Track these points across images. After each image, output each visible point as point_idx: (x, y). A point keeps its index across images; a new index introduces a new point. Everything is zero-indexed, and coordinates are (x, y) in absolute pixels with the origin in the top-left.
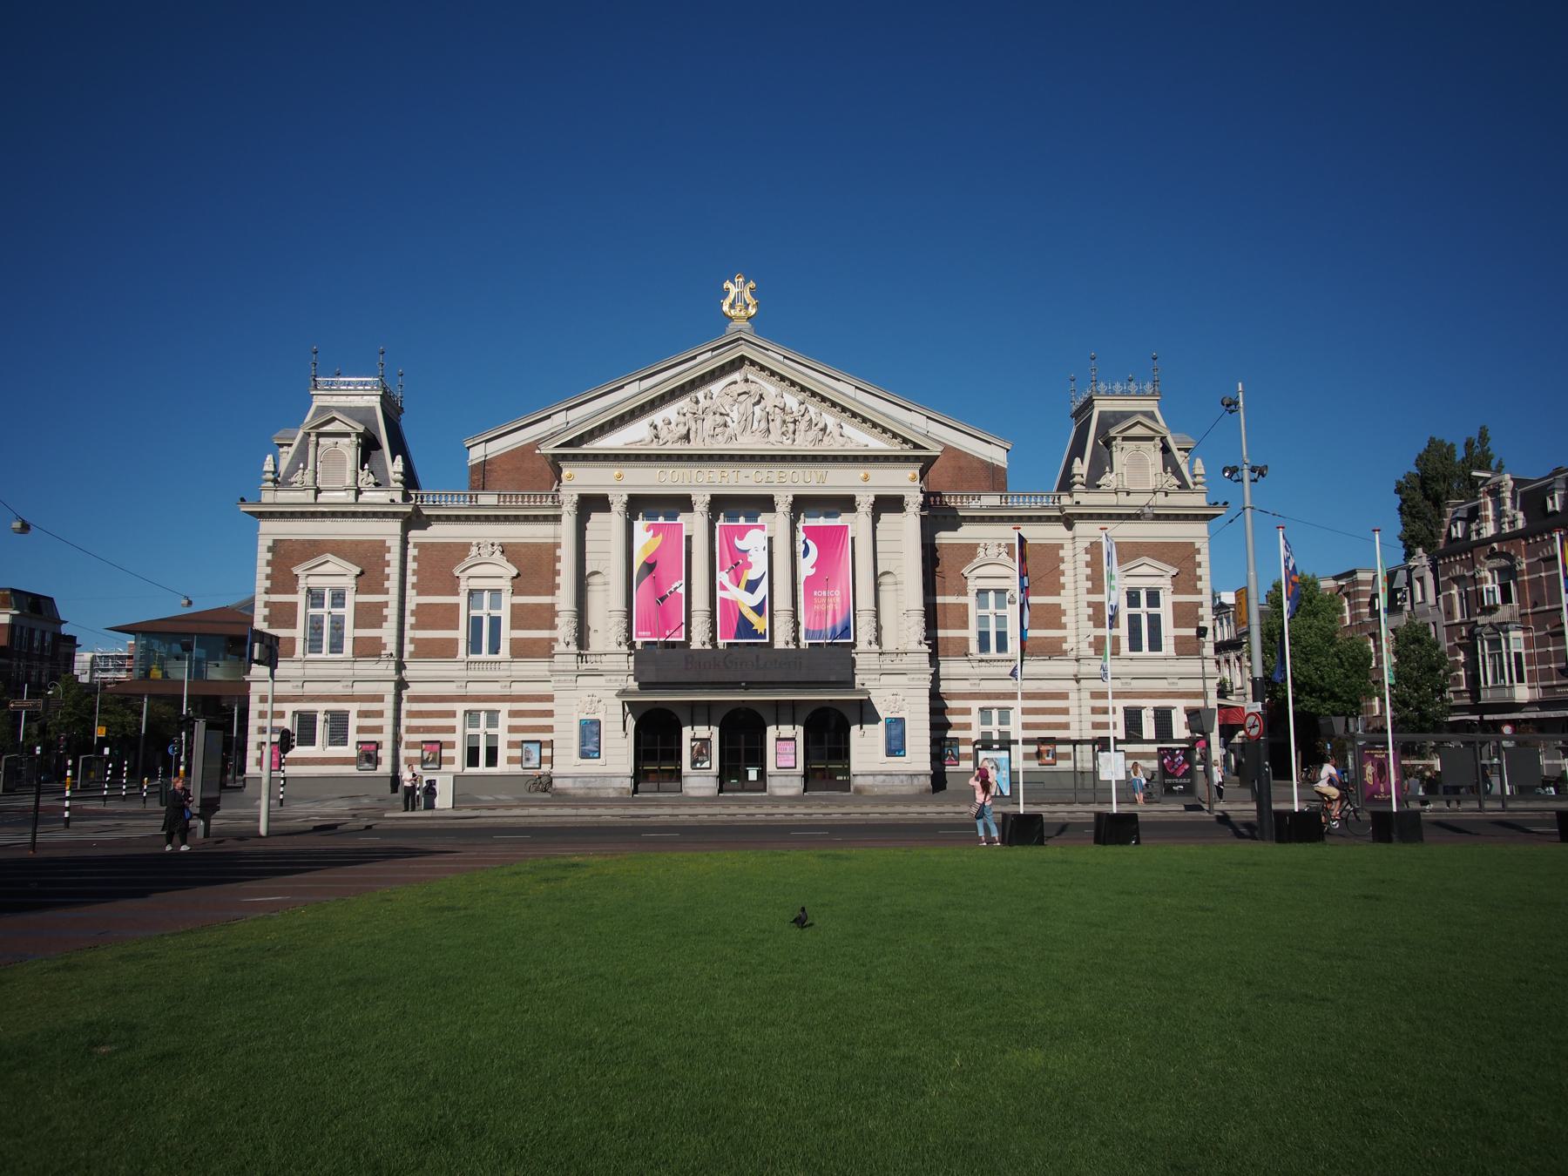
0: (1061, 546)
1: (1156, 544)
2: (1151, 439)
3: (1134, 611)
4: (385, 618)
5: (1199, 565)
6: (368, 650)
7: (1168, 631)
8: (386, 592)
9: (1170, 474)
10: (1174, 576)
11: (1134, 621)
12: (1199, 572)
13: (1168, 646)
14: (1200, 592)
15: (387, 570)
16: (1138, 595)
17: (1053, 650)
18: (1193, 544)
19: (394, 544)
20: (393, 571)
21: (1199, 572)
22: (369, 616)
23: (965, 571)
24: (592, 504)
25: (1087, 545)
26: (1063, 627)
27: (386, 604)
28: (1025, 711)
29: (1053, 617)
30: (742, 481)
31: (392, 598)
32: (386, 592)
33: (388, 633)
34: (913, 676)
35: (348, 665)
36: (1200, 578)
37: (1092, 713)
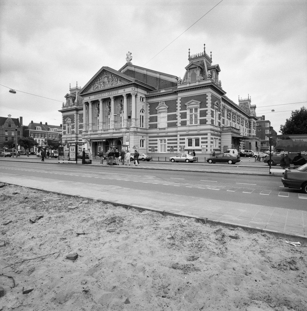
0: (177, 100)
1: (196, 96)
2: (196, 68)
3: (191, 114)
4: (74, 127)
5: (207, 100)
6: (73, 133)
7: (199, 118)
8: (74, 123)
9: (201, 76)
10: (200, 104)
11: (191, 116)
12: (207, 102)
13: (199, 122)
14: (207, 107)
15: (75, 119)
16: (192, 109)
17: (174, 125)
18: (206, 94)
19: (75, 115)
20: (75, 119)
21: (207, 102)
22: (73, 127)
23: (156, 109)
24: (87, 104)
25: (180, 98)
26: (177, 119)
27: (74, 125)
28: (168, 140)
29: (175, 117)
30: (106, 95)
31: (75, 124)
32: (74, 123)
33: (75, 130)
34: (123, 133)
35: (71, 135)
36: (207, 103)
37: (180, 140)
